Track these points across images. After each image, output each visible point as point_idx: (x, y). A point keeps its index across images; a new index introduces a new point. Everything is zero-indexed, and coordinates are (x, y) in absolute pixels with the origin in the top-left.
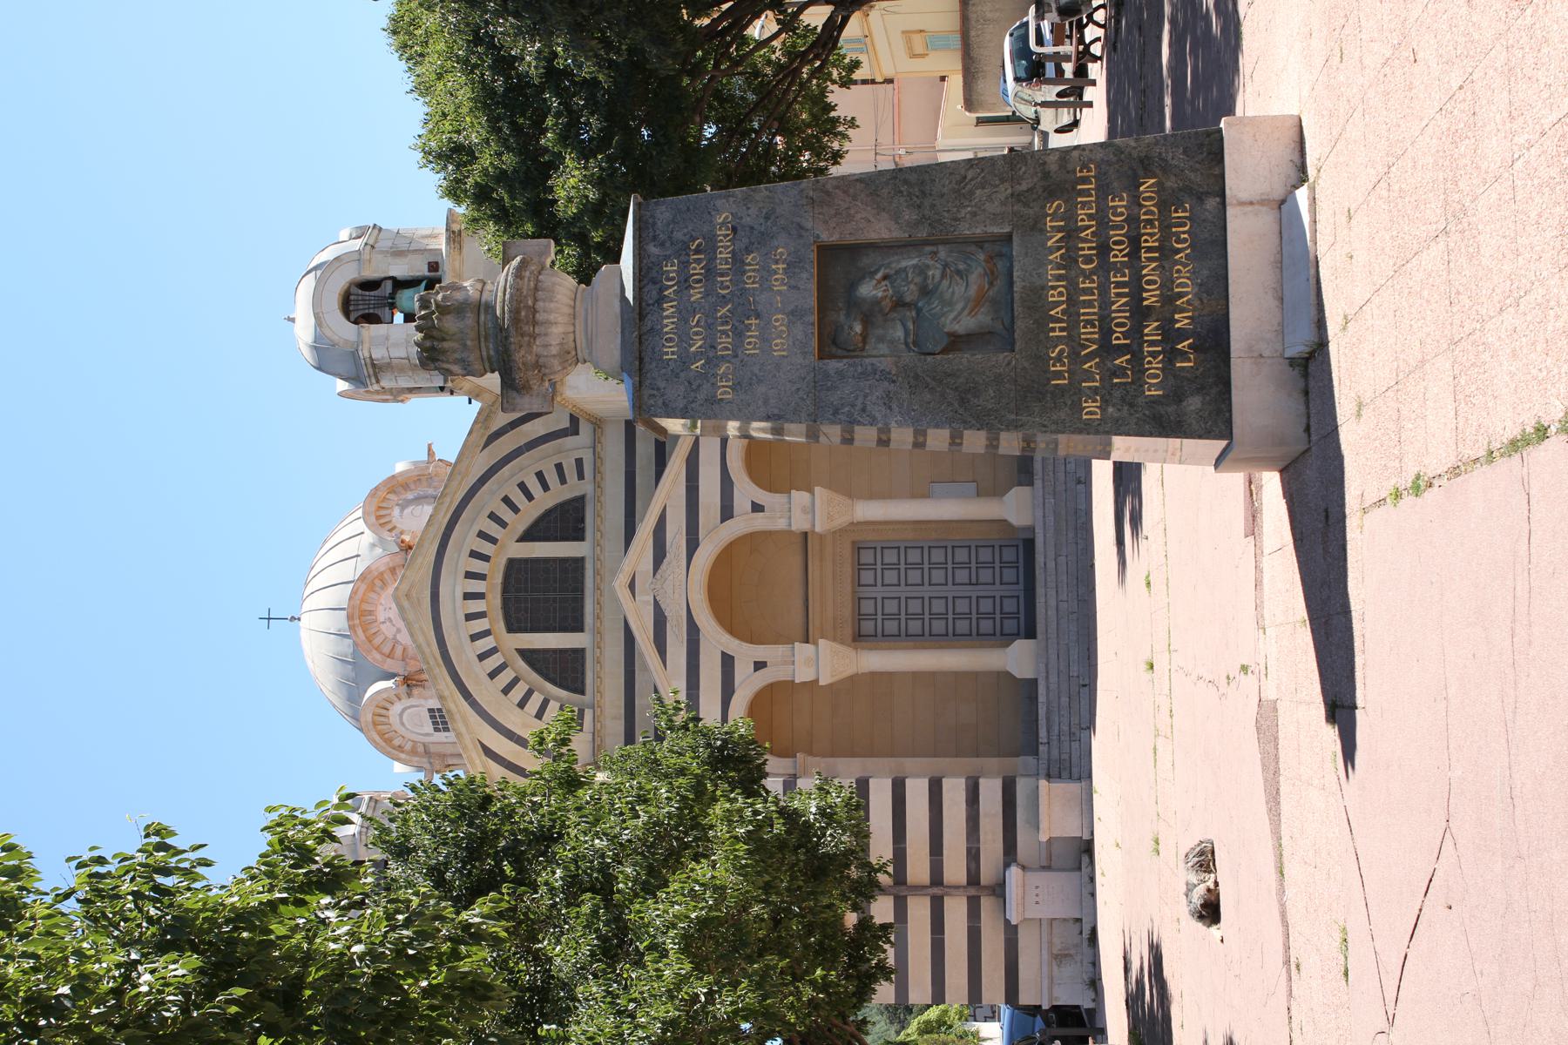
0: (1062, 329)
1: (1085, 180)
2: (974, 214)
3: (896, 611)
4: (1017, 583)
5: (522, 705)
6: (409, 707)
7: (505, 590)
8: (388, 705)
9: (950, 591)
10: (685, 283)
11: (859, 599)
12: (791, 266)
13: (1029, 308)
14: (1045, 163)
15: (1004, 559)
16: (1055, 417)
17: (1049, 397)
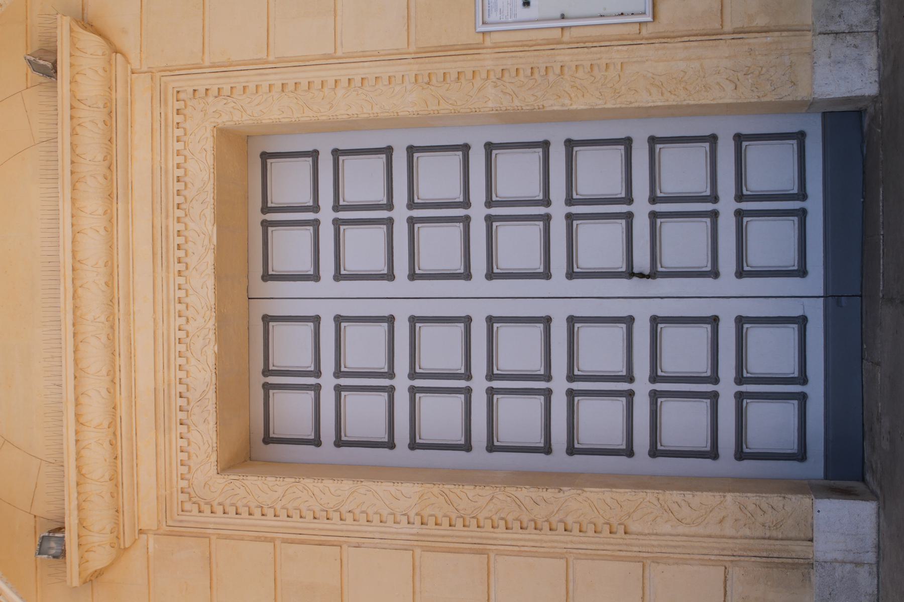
3: (381, 364)
4: (802, 272)
11: (267, 319)
15: (754, 184)
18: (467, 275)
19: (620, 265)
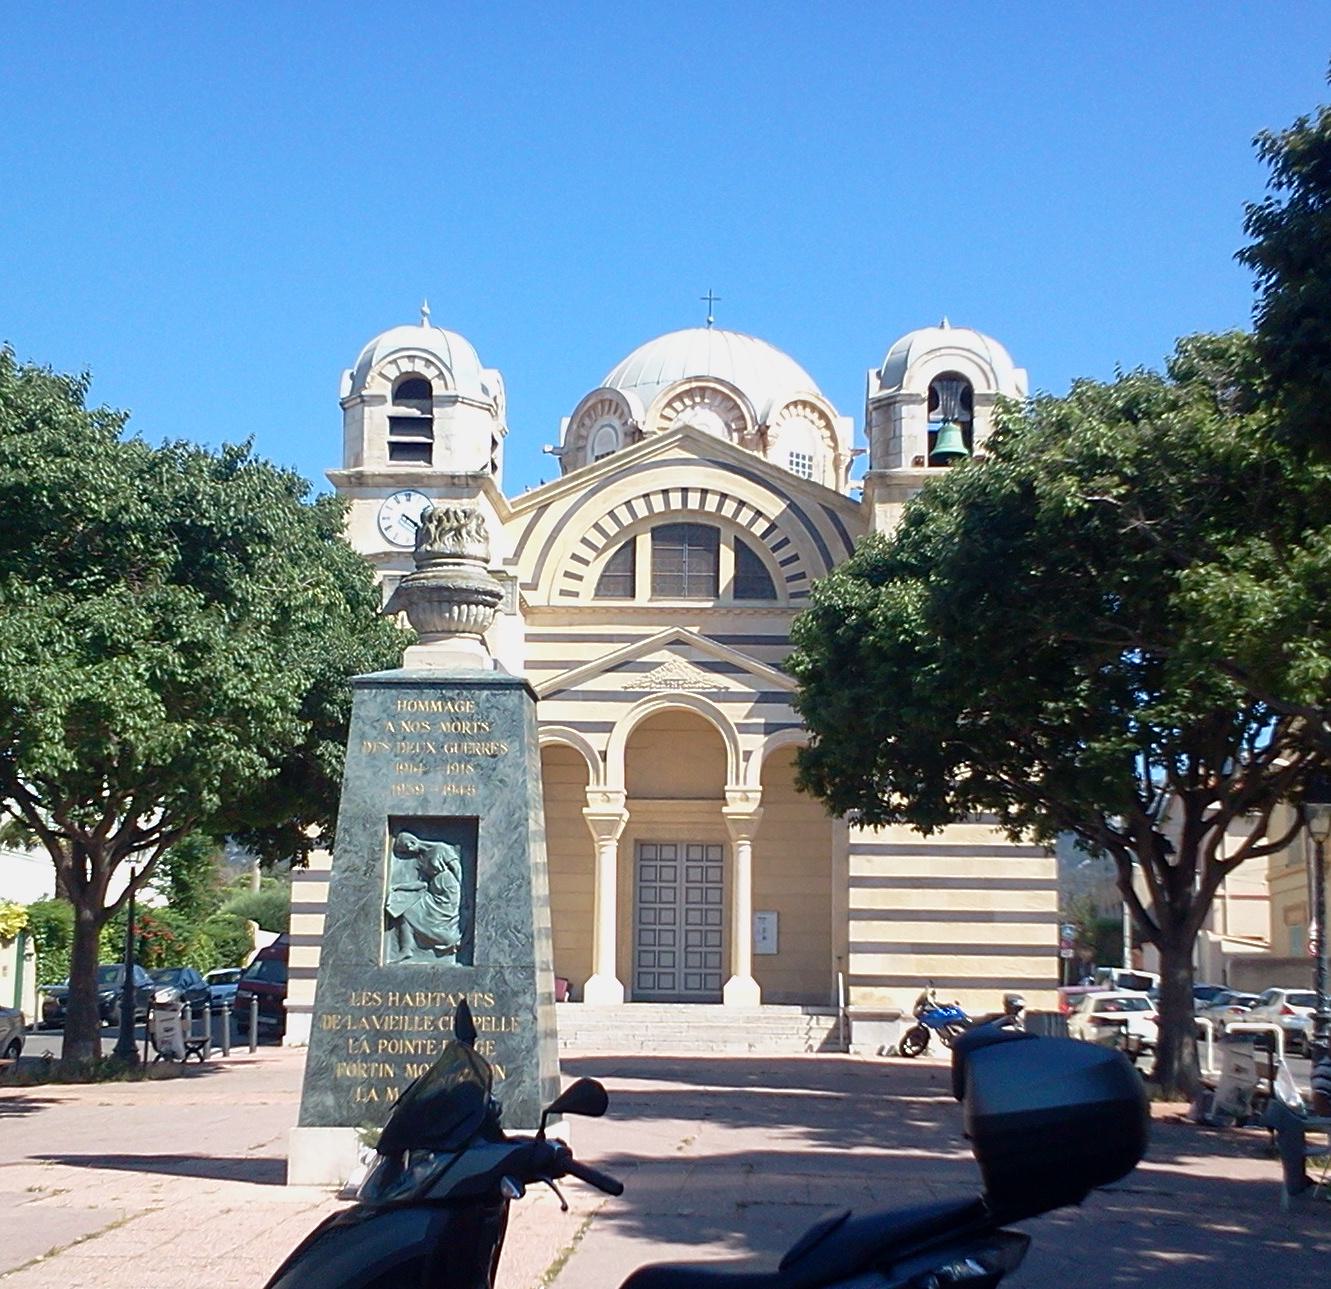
0: (394, 1002)
1: (508, 1023)
2: (489, 939)
4: (686, 988)
5: (584, 541)
6: (616, 433)
7: (690, 525)
8: (618, 414)
9: (681, 927)
10: (455, 718)
11: (675, 846)
12: (463, 799)
13: (413, 978)
14: (525, 993)
16: (328, 994)
17: (343, 990)
18: (687, 903)
19: (690, 943)
